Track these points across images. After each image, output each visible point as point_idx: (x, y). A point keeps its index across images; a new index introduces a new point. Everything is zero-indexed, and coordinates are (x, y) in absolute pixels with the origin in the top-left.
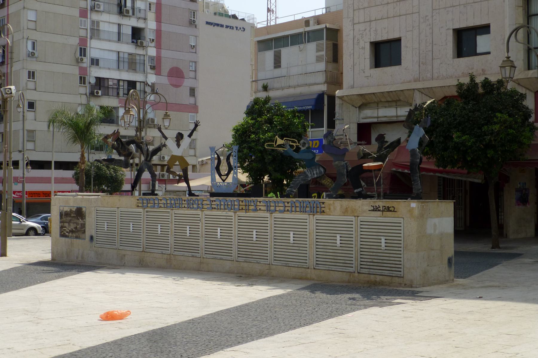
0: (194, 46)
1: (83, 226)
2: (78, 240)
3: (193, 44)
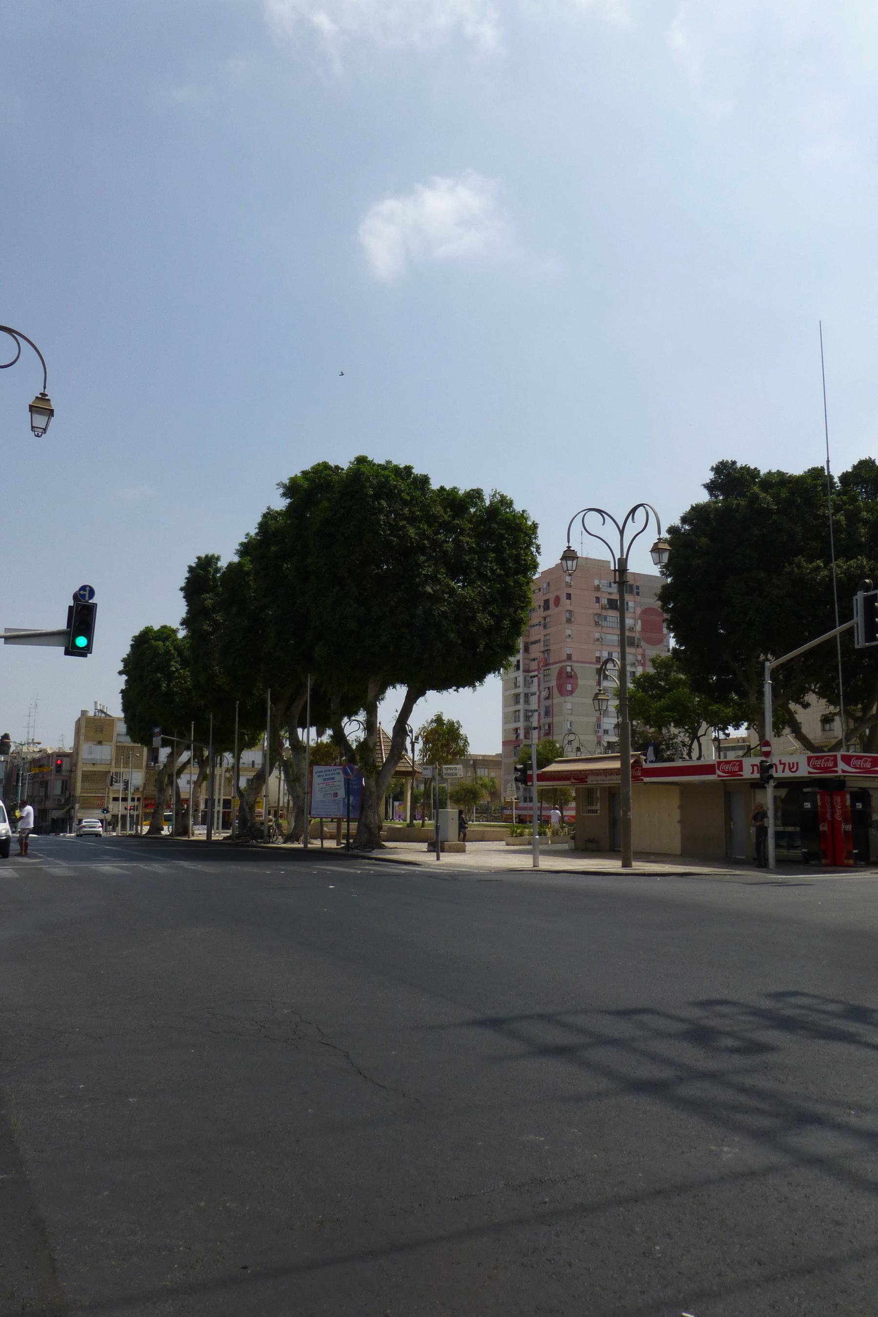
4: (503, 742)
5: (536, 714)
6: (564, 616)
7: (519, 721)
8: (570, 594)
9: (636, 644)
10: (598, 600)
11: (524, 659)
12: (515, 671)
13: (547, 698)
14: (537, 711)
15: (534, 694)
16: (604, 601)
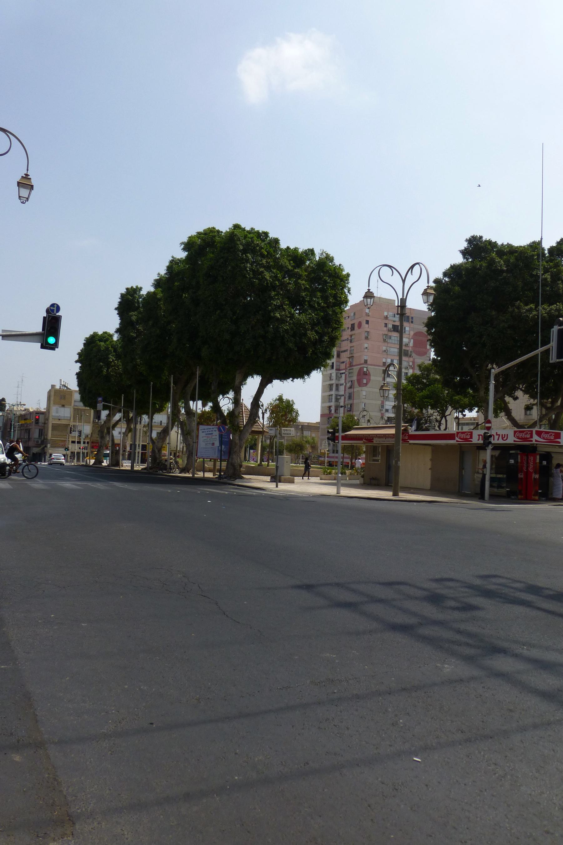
4: (321, 415)
5: (343, 398)
6: (364, 335)
7: (332, 402)
8: (368, 321)
9: (409, 355)
10: (386, 325)
11: (337, 362)
13: (351, 387)
14: (343, 395)
15: (342, 385)
16: (390, 326)
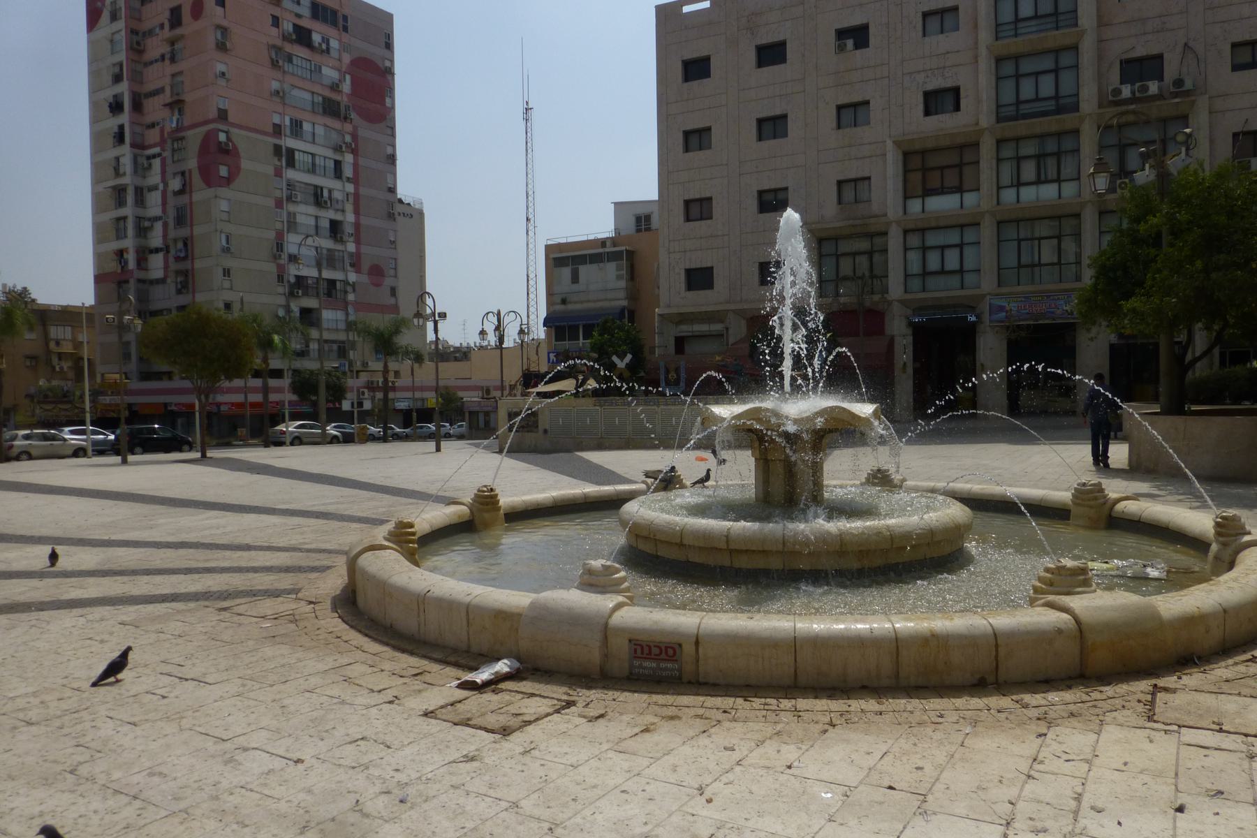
0: (394, 242)
1: (537, 421)
2: (530, 434)
3: (392, 239)
5: (158, 226)
6: (212, 38)
7: (126, 237)
10: (276, 21)
11: (132, 123)
12: (114, 147)
13: (181, 192)
14: (159, 218)
15: (155, 188)
16: (288, 27)
